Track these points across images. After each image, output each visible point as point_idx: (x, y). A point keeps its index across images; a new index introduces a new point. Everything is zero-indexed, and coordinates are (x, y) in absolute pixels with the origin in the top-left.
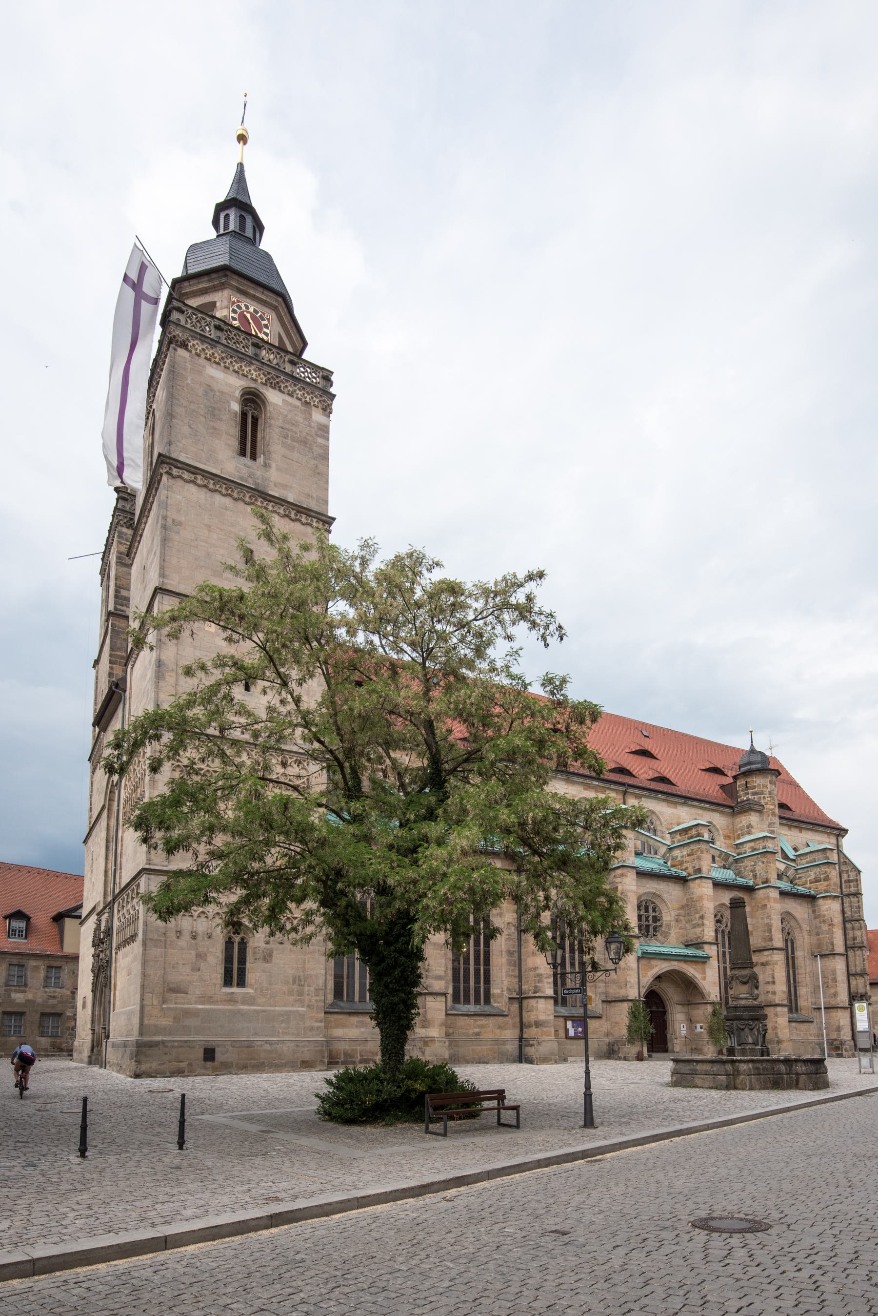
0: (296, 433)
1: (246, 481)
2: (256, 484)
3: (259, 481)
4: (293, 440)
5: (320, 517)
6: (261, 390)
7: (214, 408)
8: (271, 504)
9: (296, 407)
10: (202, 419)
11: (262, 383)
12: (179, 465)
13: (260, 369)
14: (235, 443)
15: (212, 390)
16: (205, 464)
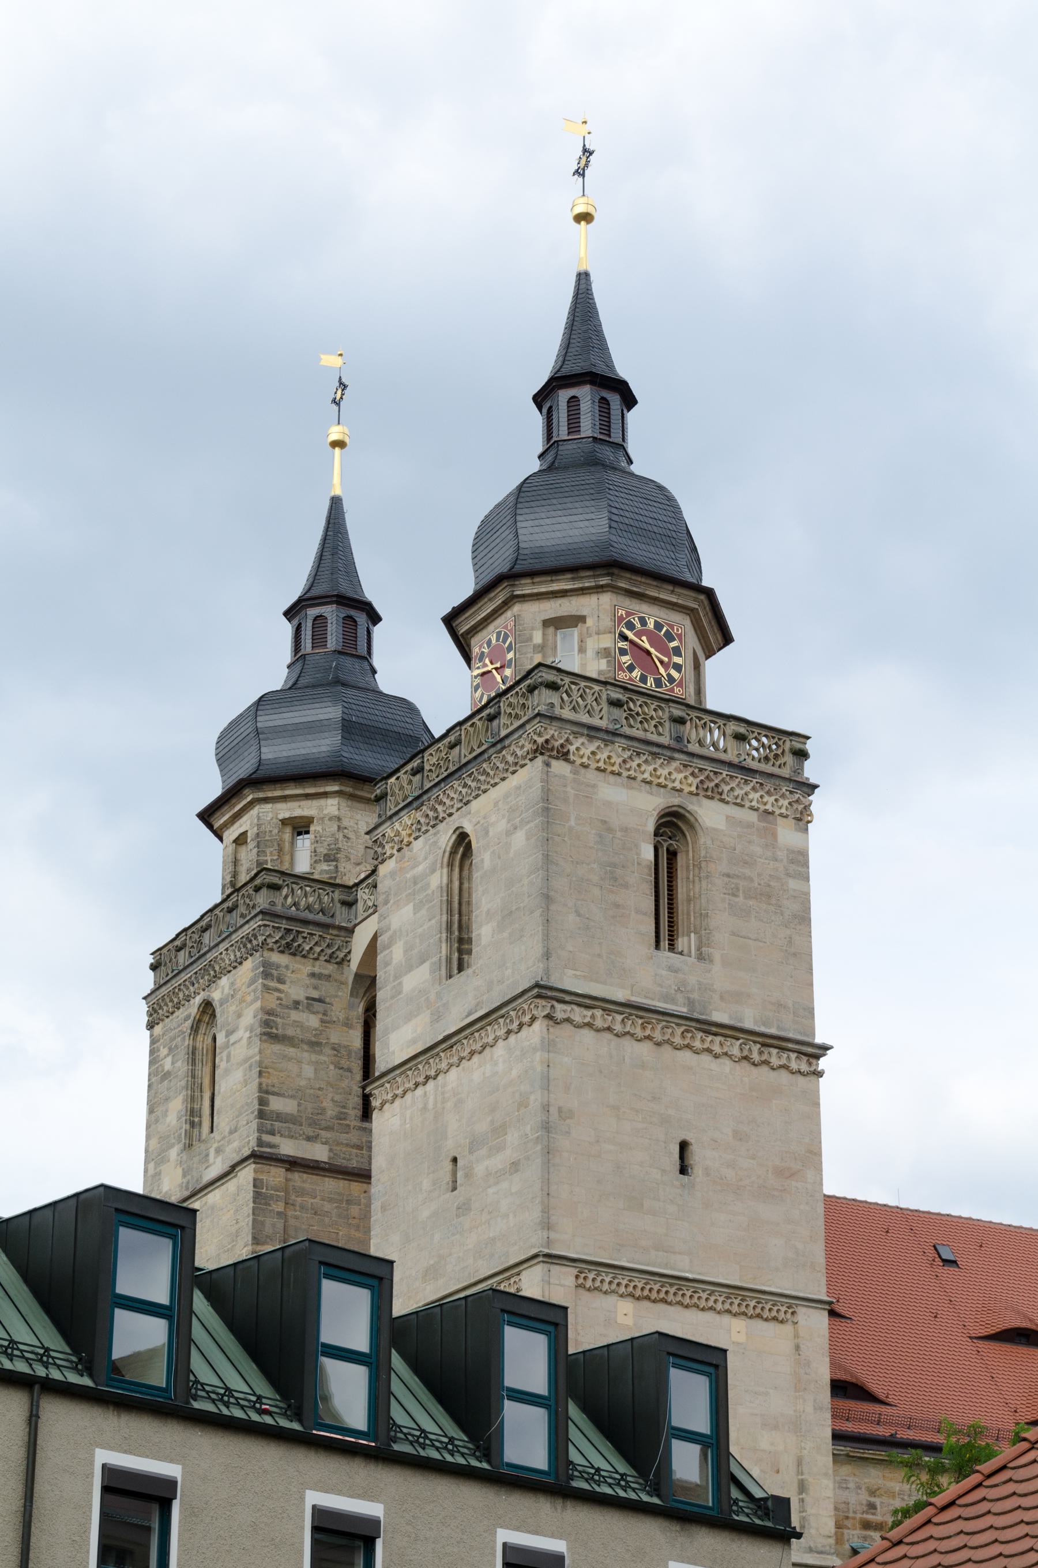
0: (751, 880)
1: (673, 1001)
2: (691, 1003)
3: (695, 996)
4: (748, 897)
5: (805, 1049)
6: (690, 807)
7: (615, 865)
8: (718, 1039)
9: (750, 826)
10: (596, 891)
11: (691, 793)
12: (568, 998)
13: (685, 766)
14: (648, 926)
15: (610, 830)
16: (605, 983)
